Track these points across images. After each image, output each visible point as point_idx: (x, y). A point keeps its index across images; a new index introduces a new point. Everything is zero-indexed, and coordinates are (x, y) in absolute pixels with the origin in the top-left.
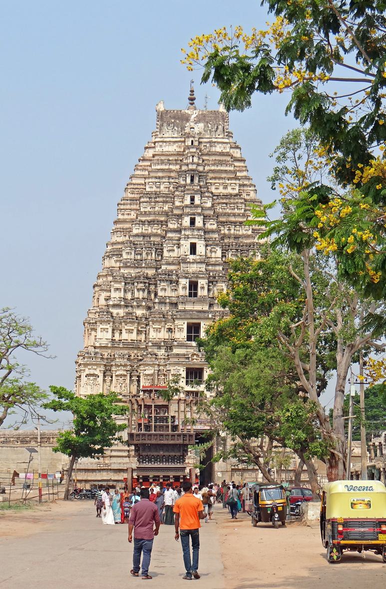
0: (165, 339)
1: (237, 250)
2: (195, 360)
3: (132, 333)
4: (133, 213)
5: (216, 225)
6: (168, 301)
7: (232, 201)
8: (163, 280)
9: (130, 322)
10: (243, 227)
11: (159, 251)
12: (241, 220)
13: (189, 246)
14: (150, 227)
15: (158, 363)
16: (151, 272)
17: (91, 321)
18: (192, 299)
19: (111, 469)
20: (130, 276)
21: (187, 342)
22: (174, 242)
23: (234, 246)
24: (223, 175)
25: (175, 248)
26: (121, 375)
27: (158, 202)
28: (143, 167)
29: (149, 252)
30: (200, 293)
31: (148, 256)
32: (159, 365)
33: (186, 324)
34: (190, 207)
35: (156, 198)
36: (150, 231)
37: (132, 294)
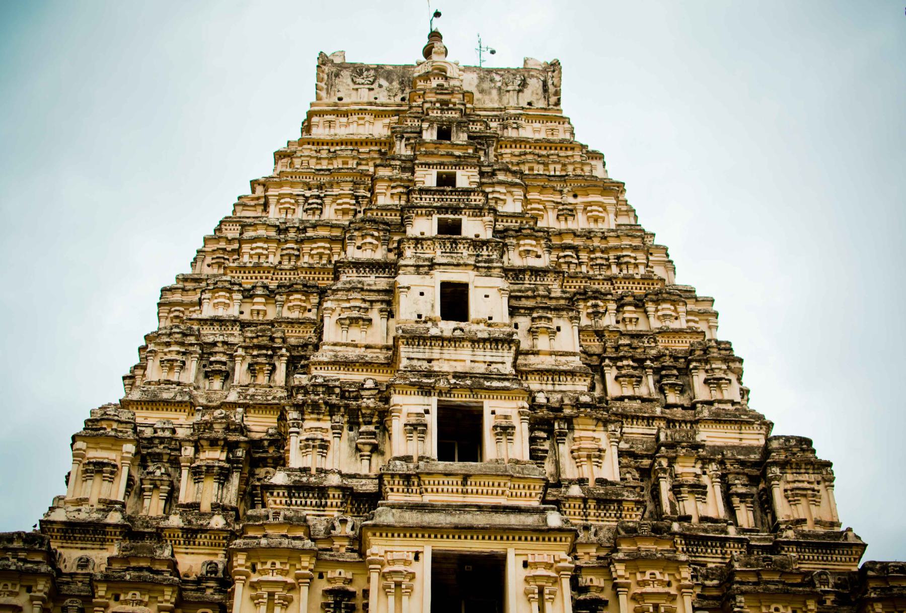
1: (640, 363)
7: (596, 243)
8: (315, 407)
10: (651, 307)
16: (261, 425)
18: (456, 466)
20: (167, 434)
22: (373, 297)
25: (374, 314)
27: (311, 240)
29: (262, 360)
30: (491, 448)
34: (435, 192)
35: (304, 230)
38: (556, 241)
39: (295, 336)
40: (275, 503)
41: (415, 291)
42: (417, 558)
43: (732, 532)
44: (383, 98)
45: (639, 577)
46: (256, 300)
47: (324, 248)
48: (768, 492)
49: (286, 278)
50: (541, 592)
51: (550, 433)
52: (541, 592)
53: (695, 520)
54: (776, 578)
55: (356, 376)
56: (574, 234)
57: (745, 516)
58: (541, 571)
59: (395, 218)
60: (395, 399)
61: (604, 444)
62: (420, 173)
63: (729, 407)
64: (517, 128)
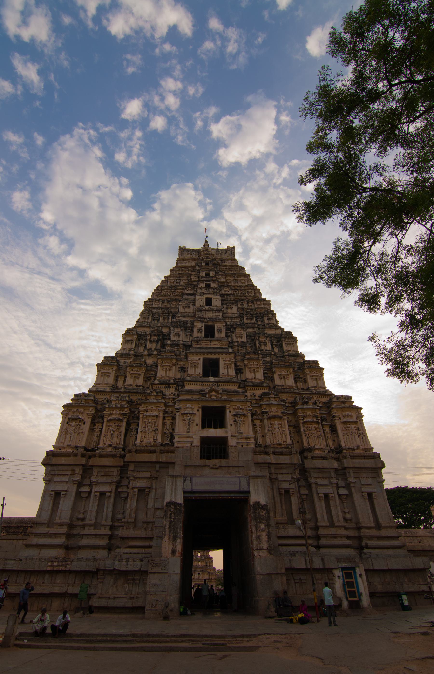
1: (252, 315)
3: (138, 378)
6: (181, 342)
7: (243, 288)
8: (177, 326)
9: (137, 367)
10: (255, 303)
13: (204, 300)
16: (165, 331)
19: (70, 572)
25: (191, 306)
26: (114, 420)
27: (177, 289)
29: (166, 316)
30: (217, 335)
31: (164, 320)
32: (166, 405)
33: (201, 360)
35: (176, 287)
36: (168, 306)
38: (233, 288)
39: (173, 311)
40: (168, 348)
41: (200, 300)
42: (199, 359)
43: (273, 353)
44: (194, 257)
48: (282, 344)
49: (172, 298)
50: (227, 367)
51: (231, 331)
52: (227, 367)
53: (264, 350)
54: (283, 363)
55: (187, 319)
56: (237, 286)
57: (276, 350)
58: (227, 362)
59: (195, 283)
60: (195, 324)
61: (243, 333)
62: (201, 273)
63: (273, 325)
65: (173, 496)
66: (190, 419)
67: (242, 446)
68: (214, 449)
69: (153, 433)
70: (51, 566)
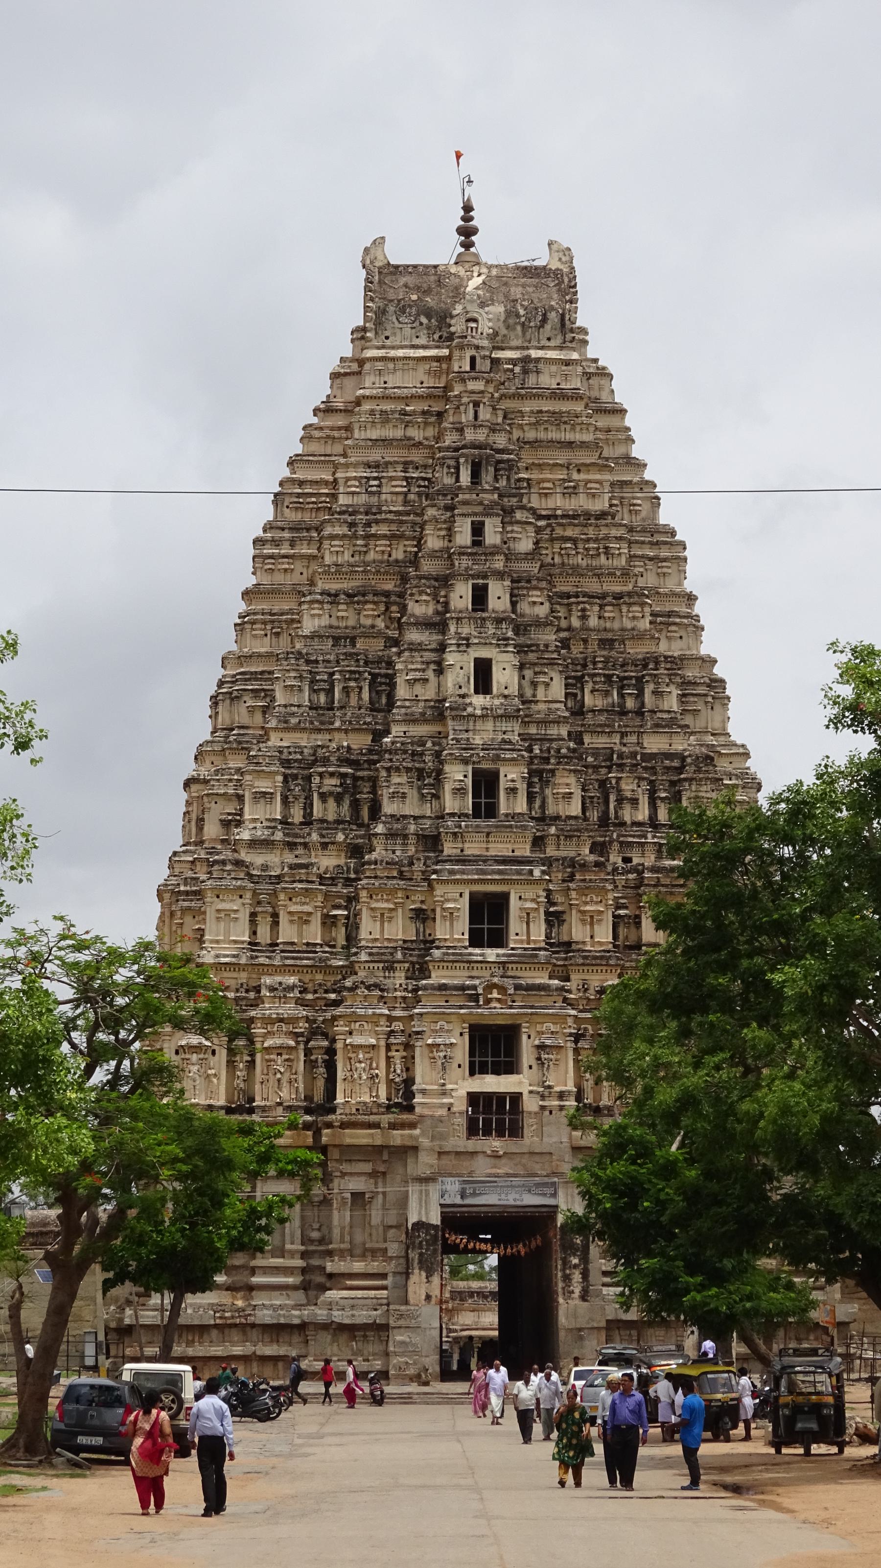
0: (405, 941)
2: (493, 1005)
3: (307, 922)
4: (298, 566)
5: (547, 605)
6: (412, 828)
8: (398, 769)
10: (624, 609)
11: (384, 684)
12: (617, 589)
14: (351, 610)
15: (387, 1012)
17: (182, 888)
19: (253, 1326)
21: (470, 950)
23: (600, 665)
24: (562, 457)
25: (430, 674)
27: (375, 536)
28: (328, 432)
29: (352, 684)
33: (467, 896)
35: (368, 524)
36: (351, 622)
37: (305, 809)
42: (461, 895)
44: (422, 341)
45: (584, 898)
46: (341, 607)
47: (385, 545)
50: (528, 914)
52: (528, 914)
58: (529, 905)
63: (665, 716)
64: (538, 372)
65: (423, 1212)
66: (445, 1057)
67: (551, 1112)
68: (494, 1116)
69: (369, 1083)
70: (220, 1318)
